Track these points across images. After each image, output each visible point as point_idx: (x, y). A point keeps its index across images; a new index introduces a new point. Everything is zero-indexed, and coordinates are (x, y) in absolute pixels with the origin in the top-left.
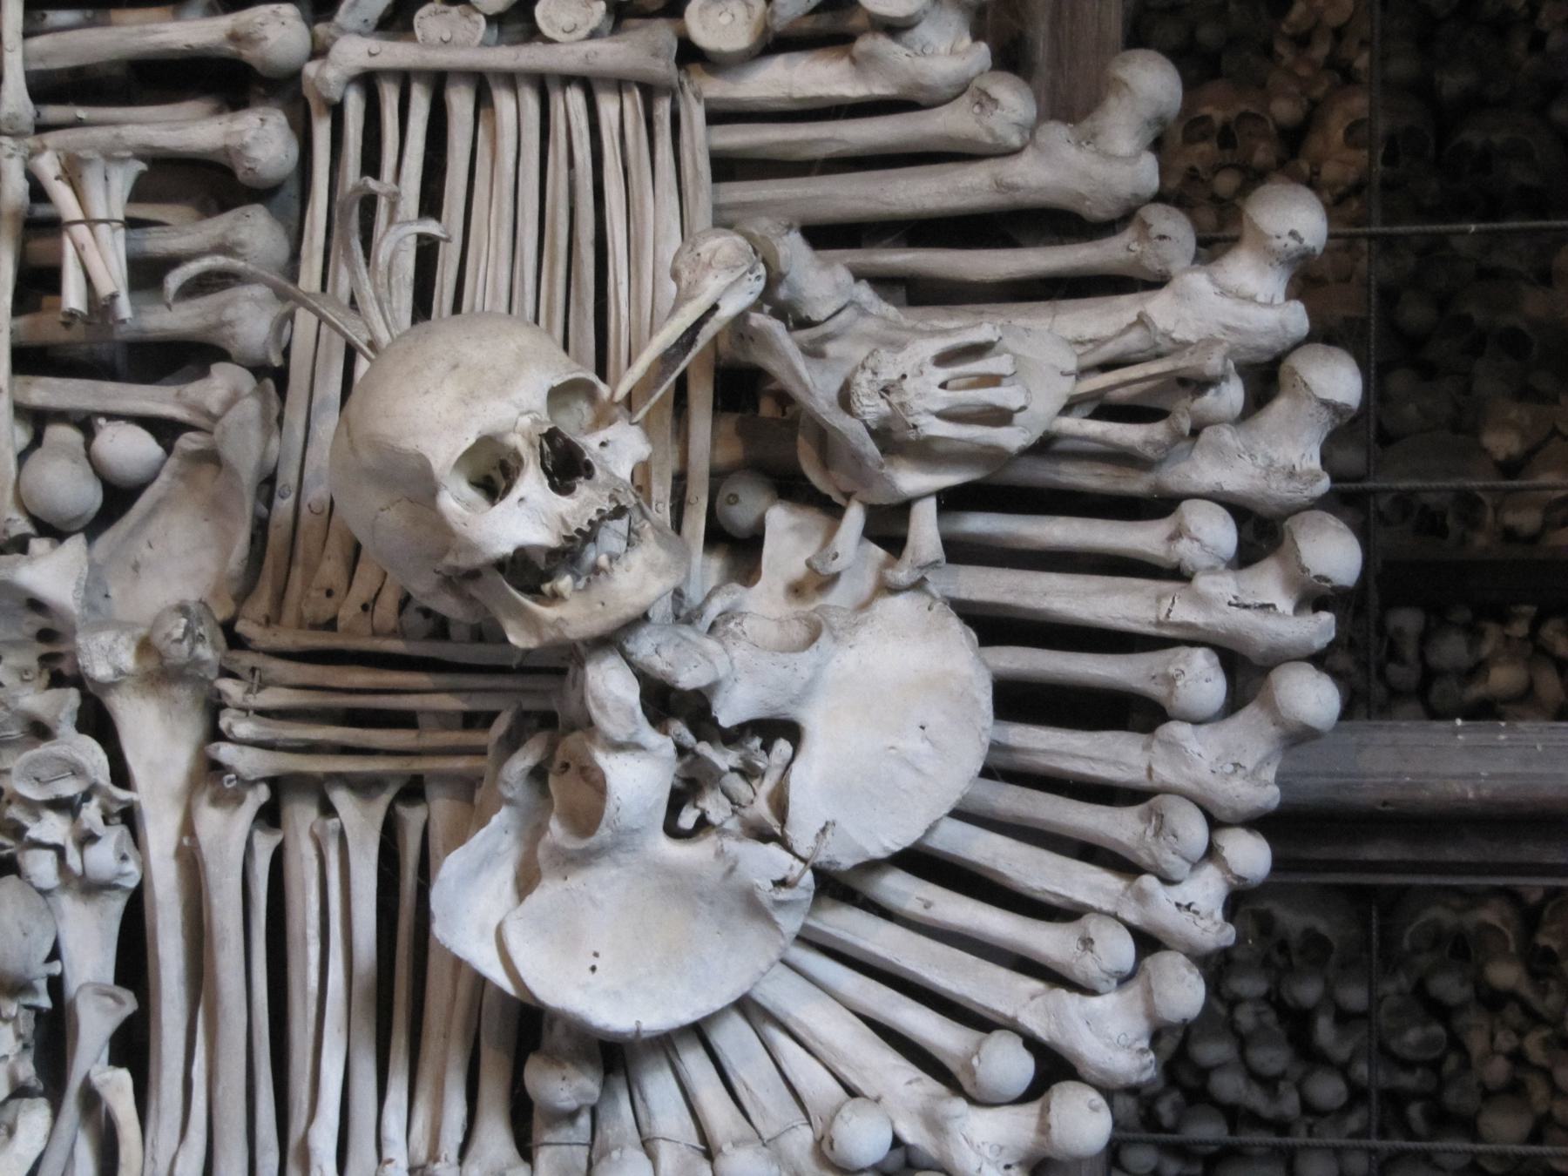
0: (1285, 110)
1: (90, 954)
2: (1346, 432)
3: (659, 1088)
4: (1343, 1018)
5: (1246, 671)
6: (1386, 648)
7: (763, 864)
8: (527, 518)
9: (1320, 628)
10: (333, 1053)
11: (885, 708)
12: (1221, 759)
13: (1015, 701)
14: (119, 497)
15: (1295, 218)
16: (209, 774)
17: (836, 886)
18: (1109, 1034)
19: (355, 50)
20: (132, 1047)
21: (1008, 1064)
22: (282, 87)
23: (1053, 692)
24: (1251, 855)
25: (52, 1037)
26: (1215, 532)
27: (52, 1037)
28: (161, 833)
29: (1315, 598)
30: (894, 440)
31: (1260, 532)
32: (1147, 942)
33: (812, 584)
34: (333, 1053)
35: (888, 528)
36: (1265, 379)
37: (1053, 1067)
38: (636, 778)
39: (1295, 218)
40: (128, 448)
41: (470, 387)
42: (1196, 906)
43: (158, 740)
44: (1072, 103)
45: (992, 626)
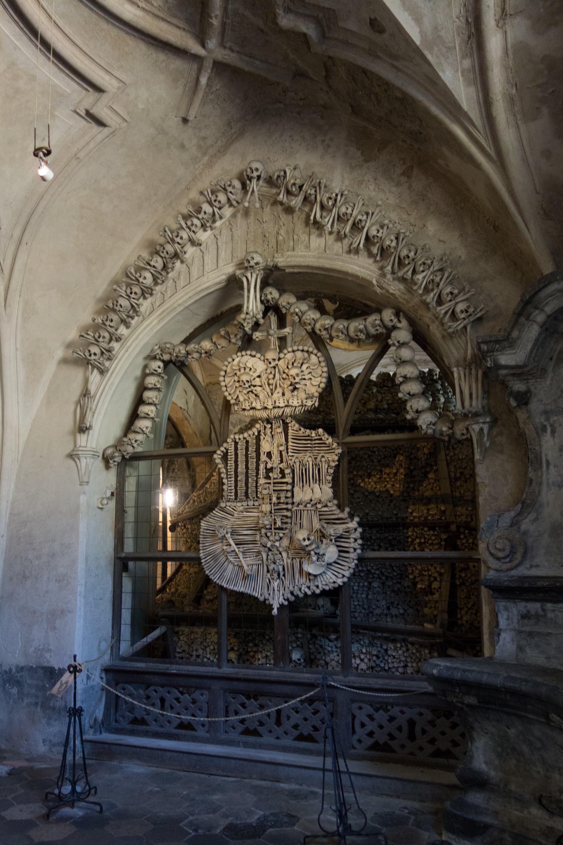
0: (394, 471)
1: (281, 569)
2: (361, 534)
3: (318, 578)
4: (396, 567)
5: (355, 550)
6: (363, 547)
7: (323, 563)
8: (307, 542)
9: (359, 546)
10: (297, 575)
11: (331, 553)
12: (353, 555)
13: (340, 551)
14: (281, 538)
15: (357, 519)
16: (288, 557)
17: (330, 564)
18: (347, 574)
19: (295, 508)
20: (284, 575)
21: (340, 576)
22: (291, 510)
23: (342, 551)
24: (356, 562)
25: (279, 575)
26: (352, 540)
27: (279, 575)
28: (285, 561)
29: (359, 544)
30: (330, 535)
31: (356, 540)
32: (349, 568)
33: (327, 544)
34: (297, 575)
35: (331, 540)
36: (356, 530)
37: (344, 576)
38: (315, 558)
39: (357, 519)
40: (281, 535)
41: (301, 535)
42: (353, 565)
43: (284, 555)
44: (342, 511)
45: (338, 546)
